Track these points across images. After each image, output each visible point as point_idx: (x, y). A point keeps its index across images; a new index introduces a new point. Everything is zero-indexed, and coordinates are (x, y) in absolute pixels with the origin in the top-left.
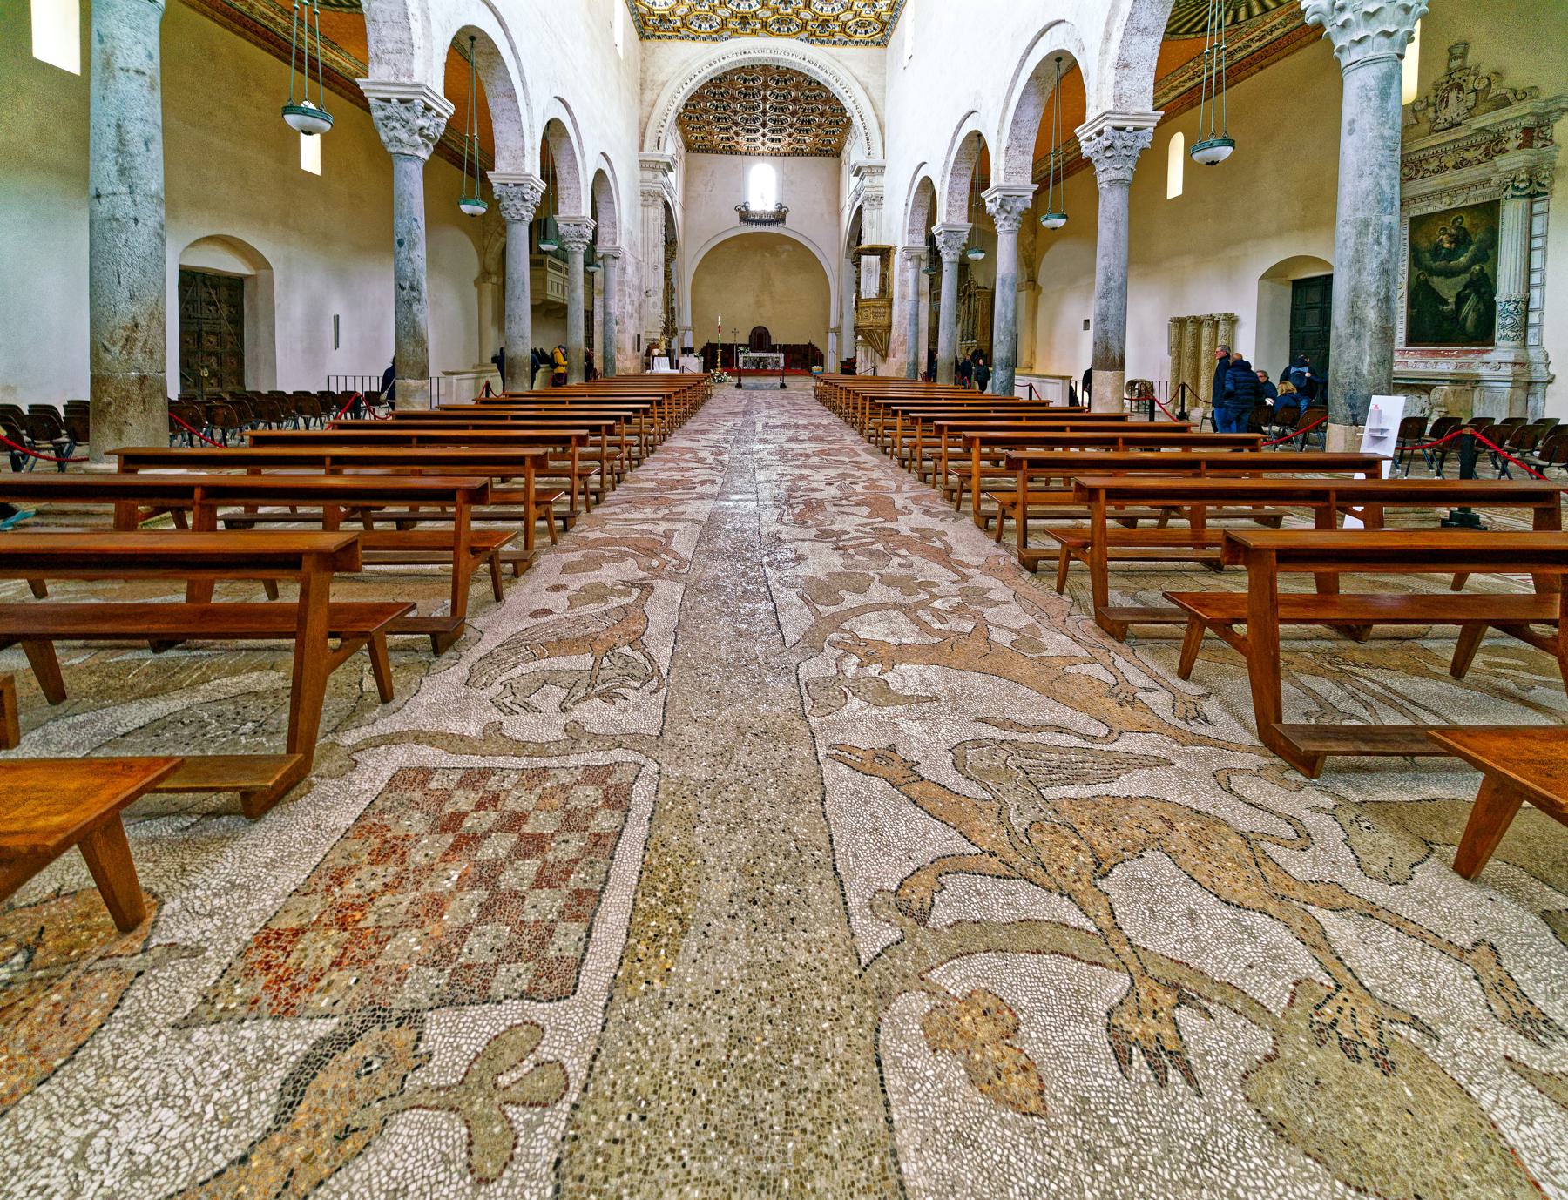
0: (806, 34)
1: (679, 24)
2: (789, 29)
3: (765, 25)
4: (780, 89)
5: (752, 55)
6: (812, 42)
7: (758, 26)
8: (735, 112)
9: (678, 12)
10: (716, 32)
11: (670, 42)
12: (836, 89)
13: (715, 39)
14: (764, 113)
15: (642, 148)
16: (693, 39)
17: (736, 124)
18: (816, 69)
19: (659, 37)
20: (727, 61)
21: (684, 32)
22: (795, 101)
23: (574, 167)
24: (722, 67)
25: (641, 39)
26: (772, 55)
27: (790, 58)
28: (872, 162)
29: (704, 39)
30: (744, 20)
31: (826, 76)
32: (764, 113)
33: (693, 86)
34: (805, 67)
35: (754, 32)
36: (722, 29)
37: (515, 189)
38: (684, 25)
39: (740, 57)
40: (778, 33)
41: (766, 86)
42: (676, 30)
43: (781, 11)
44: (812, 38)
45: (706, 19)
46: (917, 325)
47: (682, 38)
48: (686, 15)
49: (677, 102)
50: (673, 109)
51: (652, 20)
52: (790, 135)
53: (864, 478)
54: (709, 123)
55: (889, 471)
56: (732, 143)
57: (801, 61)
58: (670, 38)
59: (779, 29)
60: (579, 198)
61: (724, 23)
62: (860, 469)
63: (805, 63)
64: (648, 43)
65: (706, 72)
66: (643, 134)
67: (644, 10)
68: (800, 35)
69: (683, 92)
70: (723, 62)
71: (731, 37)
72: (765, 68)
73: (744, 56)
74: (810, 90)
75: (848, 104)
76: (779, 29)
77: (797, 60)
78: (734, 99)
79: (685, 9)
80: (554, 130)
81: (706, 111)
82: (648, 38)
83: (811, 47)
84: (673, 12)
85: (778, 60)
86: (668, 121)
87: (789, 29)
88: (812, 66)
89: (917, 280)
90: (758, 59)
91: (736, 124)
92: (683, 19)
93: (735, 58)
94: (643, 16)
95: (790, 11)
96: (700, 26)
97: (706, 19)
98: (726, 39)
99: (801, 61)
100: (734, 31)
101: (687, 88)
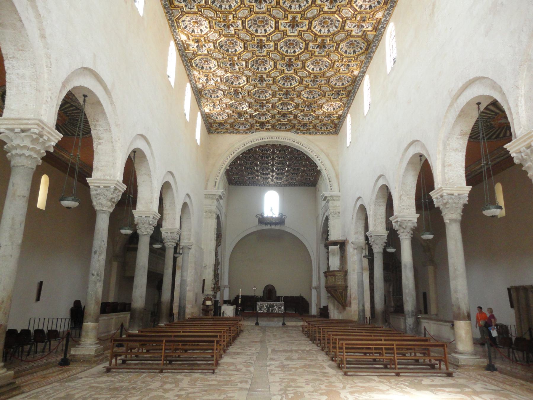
0: (295, 130)
1: (229, 126)
2: (286, 128)
3: (273, 126)
4: (281, 154)
5: (267, 140)
6: (298, 133)
7: (270, 127)
8: (257, 165)
9: (229, 122)
10: (248, 130)
11: (224, 135)
12: (312, 156)
13: (247, 133)
14: (273, 165)
15: (206, 188)
16: (236, 133)
17: (257, 171)
18: (301, 146)
19: (218, 133)
20: (253, 143)
21: (231, 130)
22: (290, 160)
23: (173, 204)
24: (250, 146)
25: (209, 133)
26: (276, 140)
27: (286, 141)
28: (333, 194)
29: (242, 133)
30: (262, 125)
31: (306, 149)
32: (273, 165)
33: (234, 155)
34: (296, 145)
35: (267, 129)
36: (251, 128)
37: (145, 219)
38: (231, 127)
39: (260, 141)
40: (280, 129)
41: (273, 153)
42: (227, 129)
43: (282, 120)
44: (298, 131)
45: (242, 124)
46: (363, 287)
47: (230, 133)
48: (233, 123)
49: (226, 163)
50: (224, 167)
51: (215, 125)
52: (287, 176)
53: (326, 381)
54: (242, 171)
55: (341, 377)
56: (255, 180)
57: (293, 142)
58: (224, 133)
59: (280, 128)
60: (174, 219)
61: (252, 126)
62: (325, 376)
63: (295, 143)
64: (212, 135)
65: (242, 148)
66: (208, 181)
67: (211, 121)
68: (292, 130)
69: (229, 159)
70: (251, 144)
71: (255, 132)
72: (274, 146)
73: (262, 141)
74: (298, 155)
75: (318, 163)
76: (280, 128)
77: (290, 142)
78: (257, 159)
79: (232, 120)
80: (166, 187)
81: (241, 165)
82: (212, 133)
83: (298, 135)
84: (226, 121)
85: (280, 142)
86: (221, 174)
87: (286, 128)
88: (298, 145)
89: (361, 261)
90: (270, 141)
91: (257, 171)
92: (231, 124)
93: (258, 142)
94: (210, 124)
95: (286, 120)
96: (239, 127)
97: (242, 124)
98: (253, 132)
99: (293, 142)
100: (257, 129)
101: (231, 157)
